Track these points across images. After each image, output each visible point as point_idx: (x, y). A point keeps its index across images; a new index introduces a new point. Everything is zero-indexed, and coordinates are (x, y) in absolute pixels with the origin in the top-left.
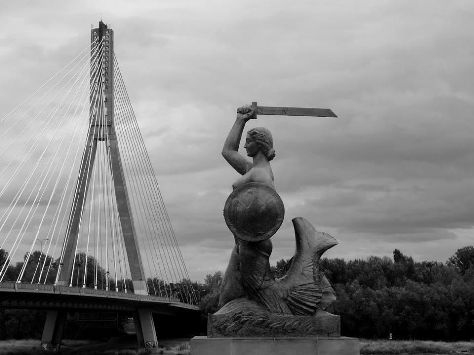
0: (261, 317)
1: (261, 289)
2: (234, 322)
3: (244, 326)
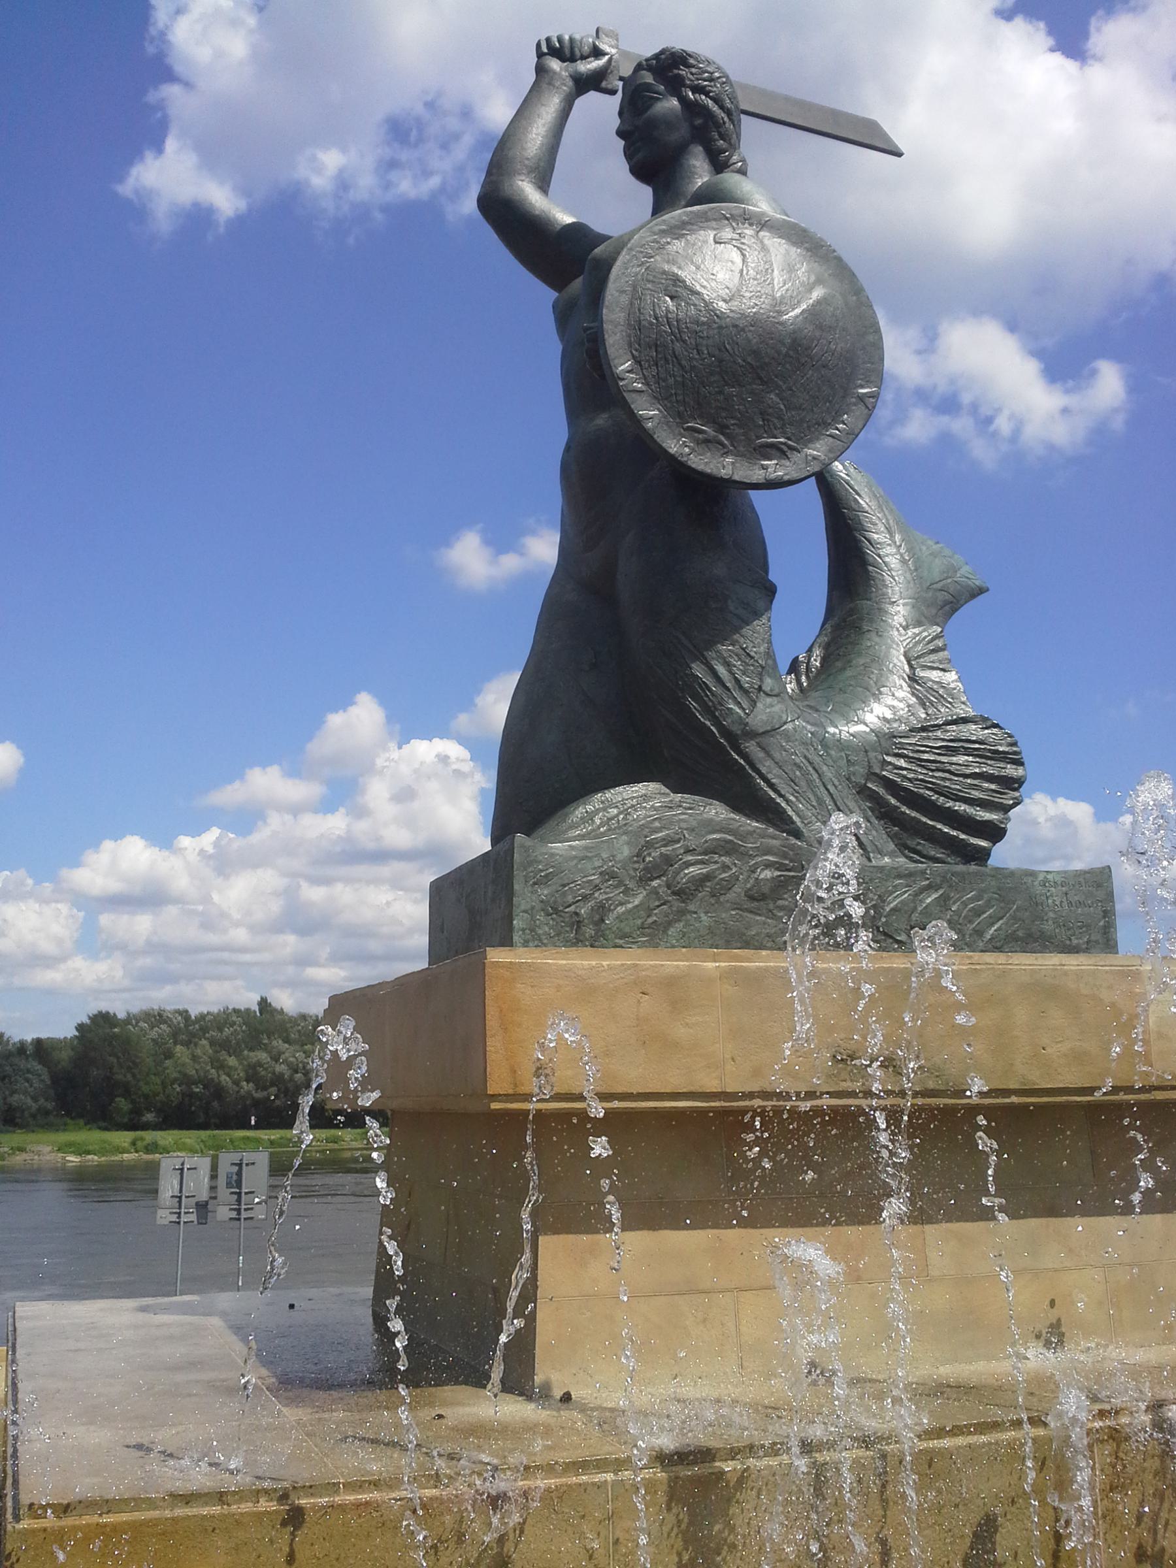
0: (768, 865)
1: (752, 735)
2: (643, 881)
3: (692, 907)
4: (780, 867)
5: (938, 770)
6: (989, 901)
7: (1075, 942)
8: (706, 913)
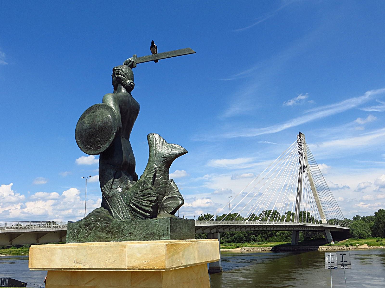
0: (105, 223)
4: (107, 223)
5: (141, 200)
6: (144, 227)
7: (161, 234)
8: (94, 233)
